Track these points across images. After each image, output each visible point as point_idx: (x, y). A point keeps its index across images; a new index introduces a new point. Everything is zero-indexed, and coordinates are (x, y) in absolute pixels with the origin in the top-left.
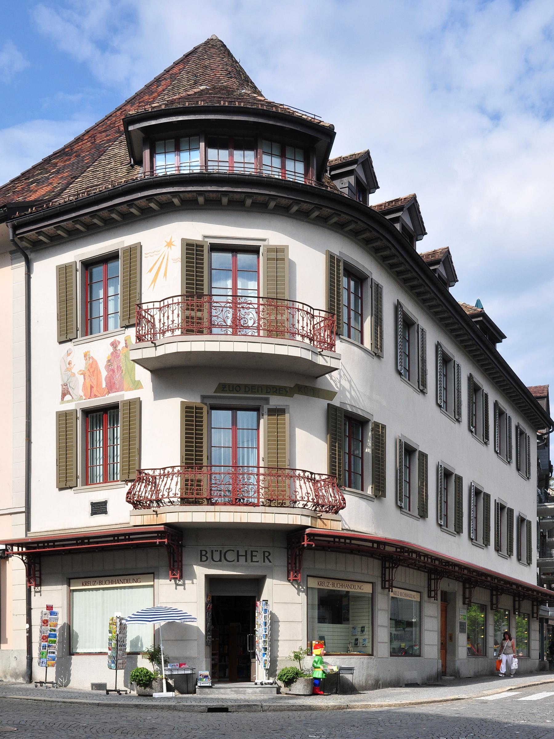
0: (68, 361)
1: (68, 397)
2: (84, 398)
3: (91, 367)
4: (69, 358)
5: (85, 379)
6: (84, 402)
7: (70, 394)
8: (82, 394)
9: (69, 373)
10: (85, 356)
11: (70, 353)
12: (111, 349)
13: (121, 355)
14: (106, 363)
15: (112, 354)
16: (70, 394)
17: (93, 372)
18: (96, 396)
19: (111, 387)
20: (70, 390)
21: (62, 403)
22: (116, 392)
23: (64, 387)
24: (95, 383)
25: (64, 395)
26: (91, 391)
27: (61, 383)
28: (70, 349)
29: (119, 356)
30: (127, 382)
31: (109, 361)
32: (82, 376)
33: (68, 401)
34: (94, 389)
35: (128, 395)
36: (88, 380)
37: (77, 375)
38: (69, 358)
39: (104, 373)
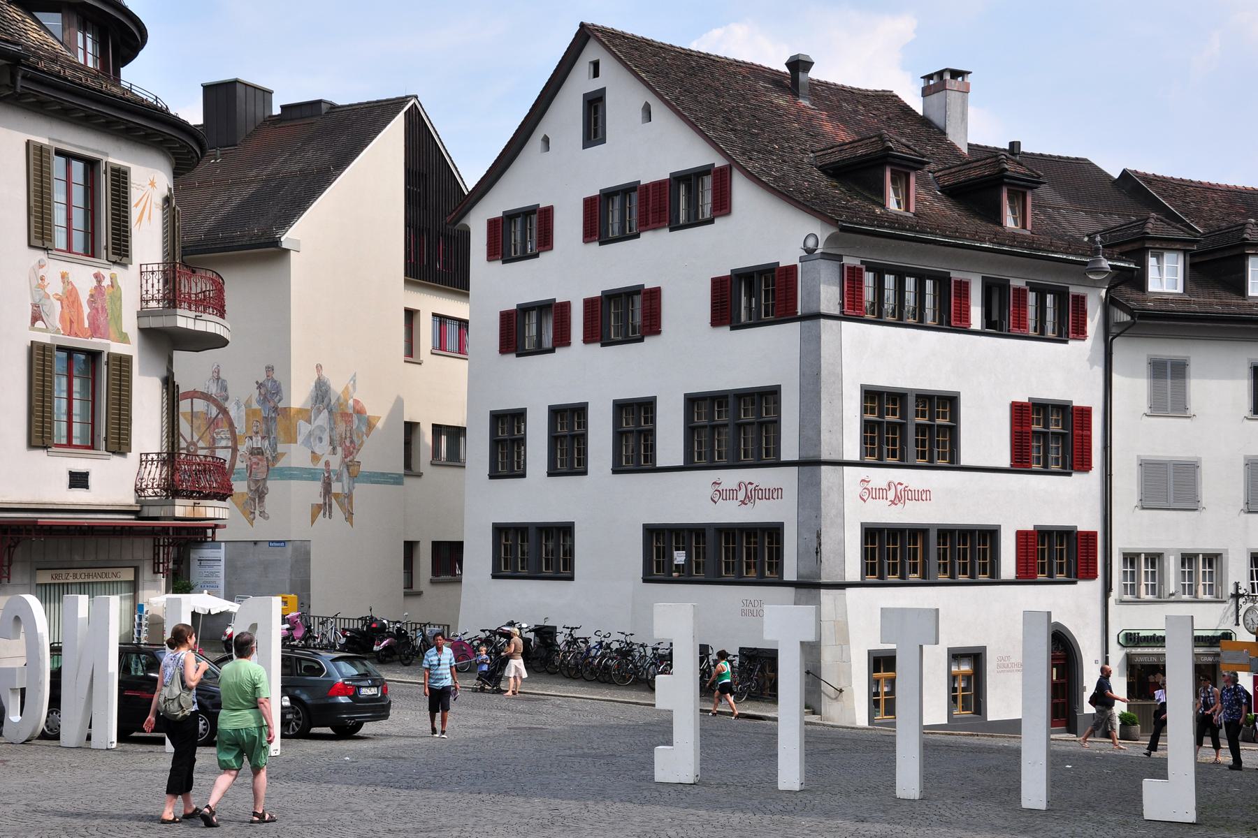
0: (40, 275)
1: (39, 324)
2: (62, 332)
3: (71, 295)
4: (41, 272)
5: (62, 307)
6: (62, 338)
7: (43, 320)
8: (60, 326)
9: (42, 292)
10: (64, 276)
11: (43, 266)
12: (95, 283)
13: (106, 294)
14: (88, 297)
15: (96, 288)
16: (43, 320)
17: (73, 302)
18: (77, 335)
19: (95, 331)
20: (43, 314)
21: (33, 330)
22: (100, 338)
23: (36, 308)
24: (76, 318)
25: (36, 318)
26: (71, 325)
27: (30, 301)
28: (42, 260)
29: (103, 295)
30: (112, 329)
31: (92, 296)
32: (59, 302)
33: (40, 330)
34: (75, 325)
35: (117, 348)
36: (66, 311)
37: (52, 298)
38: (41, 272)
39: (86, 310)
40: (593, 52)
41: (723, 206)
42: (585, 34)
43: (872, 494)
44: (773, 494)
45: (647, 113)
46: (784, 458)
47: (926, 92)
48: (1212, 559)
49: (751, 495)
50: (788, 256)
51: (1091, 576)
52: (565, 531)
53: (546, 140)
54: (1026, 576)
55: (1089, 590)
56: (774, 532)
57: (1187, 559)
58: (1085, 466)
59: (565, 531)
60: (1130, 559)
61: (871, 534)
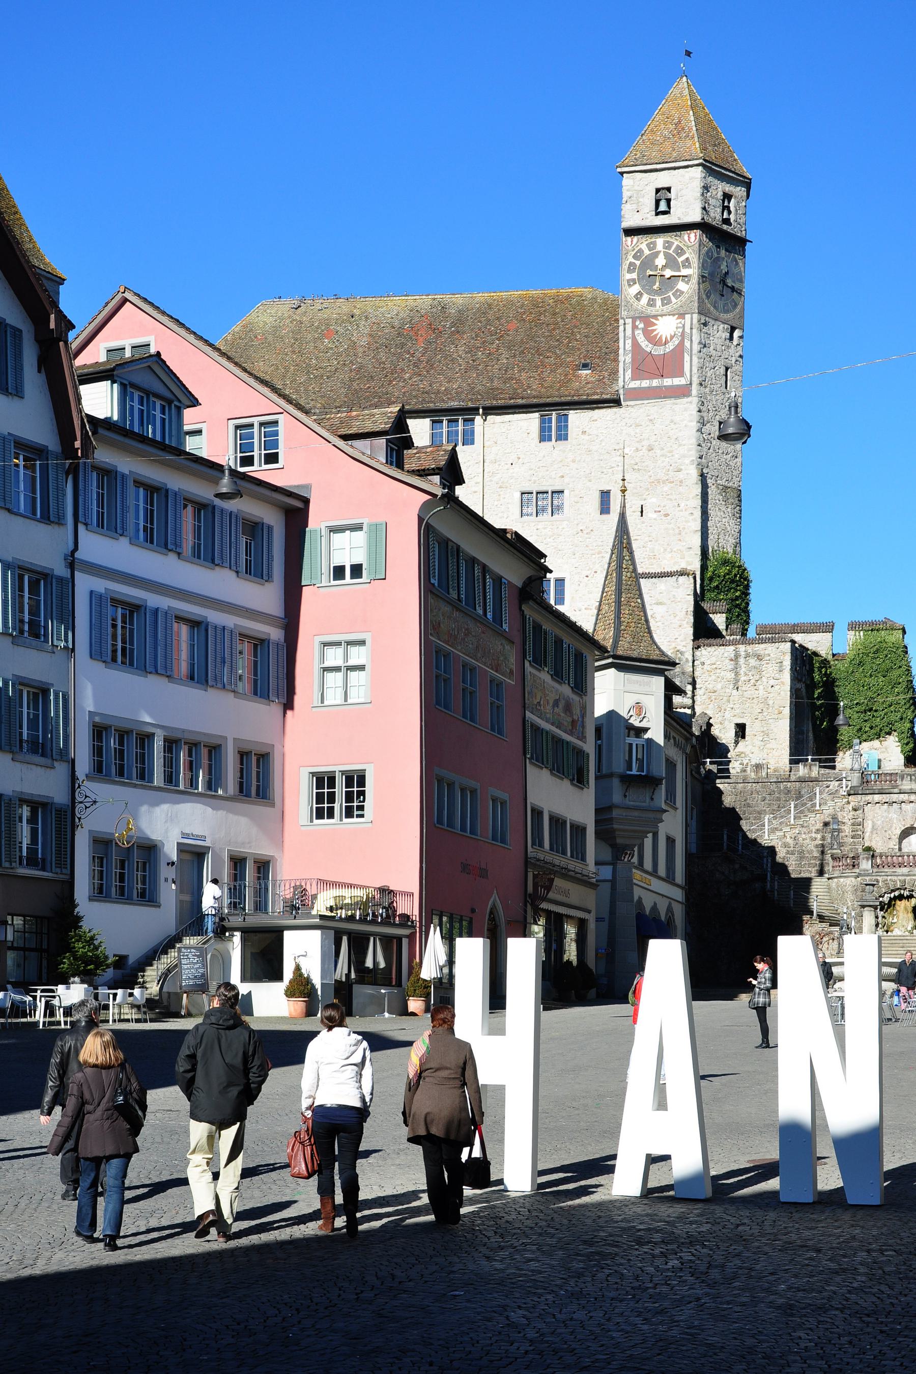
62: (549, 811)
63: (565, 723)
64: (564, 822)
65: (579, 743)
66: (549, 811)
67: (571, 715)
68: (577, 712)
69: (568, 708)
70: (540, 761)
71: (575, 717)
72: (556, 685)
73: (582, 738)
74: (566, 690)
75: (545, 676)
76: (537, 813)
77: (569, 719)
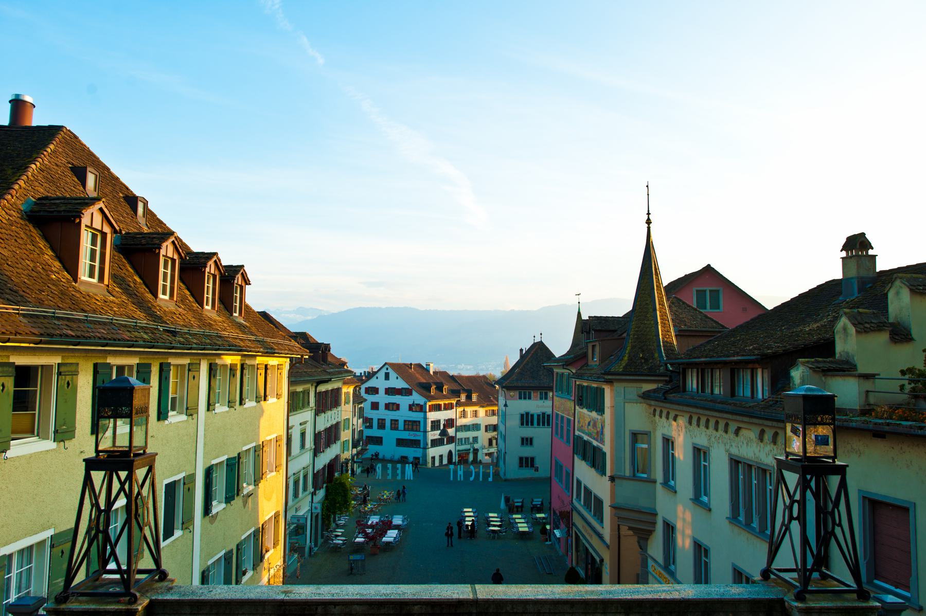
40: (387, 366)
41: (411, 394)
42: (386, 364)
43: (432, 435)
44: (420, 436)
45: (397, 378)
46: (421, 430)
47: (426, 365)
48: (468, 438)
49: (415, 435)
50: (422, 403)
51: (454, 442)
52: (381, 438)
53: (377, 378)
54: (447, 444)
55: (454, 444)
56: (419, 441)
57: (465, 439)
58: (453, 427)
59: (381, 438)
60: (458, 439)
61: (432, 441)
62: (584, 484)
63: (594, 434)
64: (591, 493)
65: (601, 445)
66: (584, 484)
67: (597, 429)
68: (599, 426)
69: (595, 425)
70: (584, 458)
71: (598, 430)
72: (589, 413)
73: (602, 442)
74: (594, 414)
75: (585, 411)
76: (579, 482)
77: (595, 431)
